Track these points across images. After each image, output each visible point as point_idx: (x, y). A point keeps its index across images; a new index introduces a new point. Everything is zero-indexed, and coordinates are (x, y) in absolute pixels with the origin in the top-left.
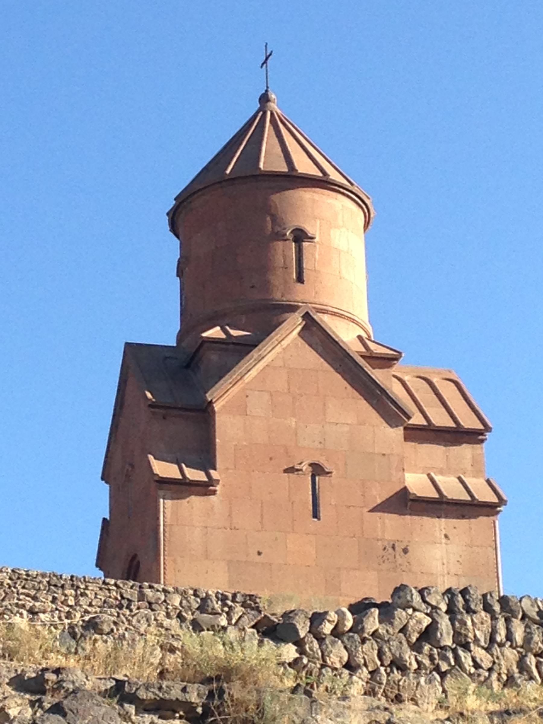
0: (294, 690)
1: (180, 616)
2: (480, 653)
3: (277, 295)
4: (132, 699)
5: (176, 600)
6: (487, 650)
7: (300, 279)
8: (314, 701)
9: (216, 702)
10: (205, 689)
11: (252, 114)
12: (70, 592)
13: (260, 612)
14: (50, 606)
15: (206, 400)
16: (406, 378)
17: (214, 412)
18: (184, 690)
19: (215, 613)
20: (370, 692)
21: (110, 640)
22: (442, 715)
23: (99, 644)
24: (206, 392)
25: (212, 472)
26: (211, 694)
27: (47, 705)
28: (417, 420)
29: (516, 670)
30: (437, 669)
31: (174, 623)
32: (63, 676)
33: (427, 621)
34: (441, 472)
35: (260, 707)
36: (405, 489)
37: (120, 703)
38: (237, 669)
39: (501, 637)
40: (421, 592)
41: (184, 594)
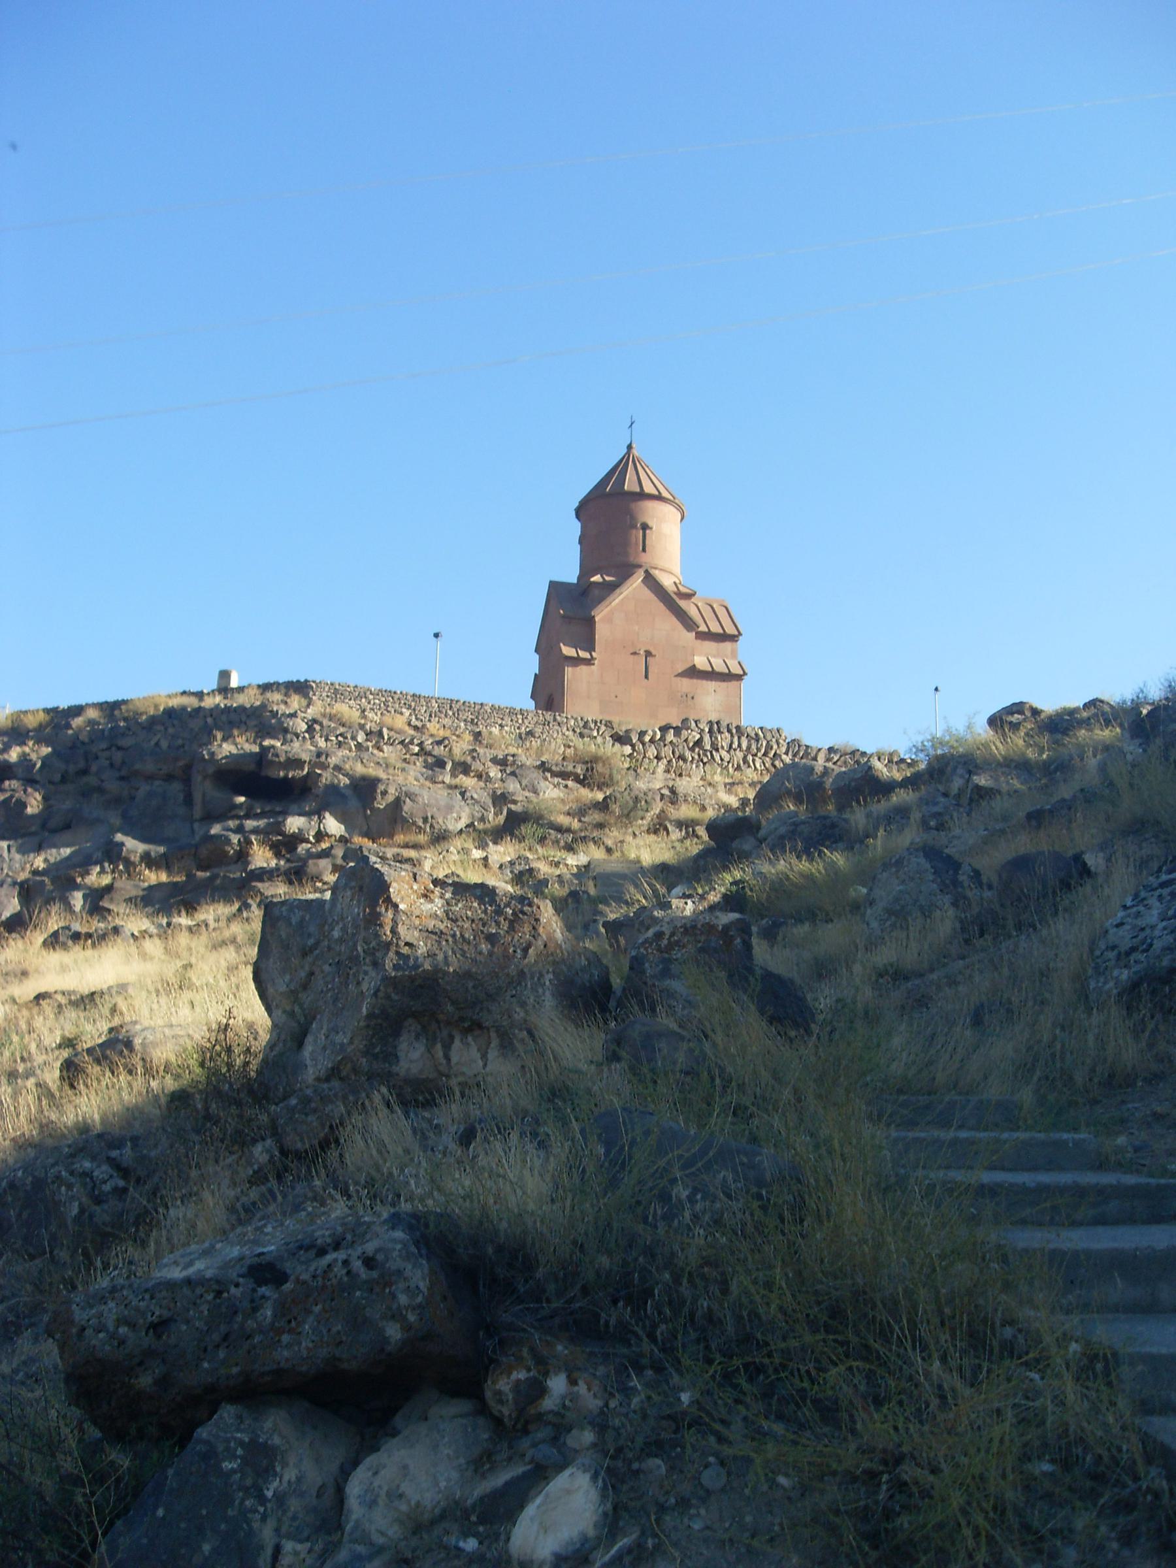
0: (628, 769)
1: (573, 730)
2: (724, 753)
3: (632, 559)
4: (549, 770)
5: (572, 722)
6: (728, 752)
7: (644, 550)
8: (637, 775)
9: (590, 773)
10: (584, 767)
11: (621, 457)
12: (520, 717)
13: (613, 728)
14: (510, 723)
15: (590, 613)
16: (699, 605)
17: (595, 622)
18: (574, 767)
19: (591, 729)
20: (667, 771)
21: (539, 741)
22: (701, 783)
23: (533, 743)
24: (592, 610)
25: (593, 653)
26: (587, 769)
27: (508, 772)
28: (703, 628)
29: (741, 763)
30: (702, 761)
31: (570, 733)
32: (516, 758)
33: (698, 736)
34: (714, 656)
35: (611, 776)
36: (694, 665)
37: (543, 772)
38: (601, 758)
39: (735, 745)
40: (696, 722)
41: (576, 719)
